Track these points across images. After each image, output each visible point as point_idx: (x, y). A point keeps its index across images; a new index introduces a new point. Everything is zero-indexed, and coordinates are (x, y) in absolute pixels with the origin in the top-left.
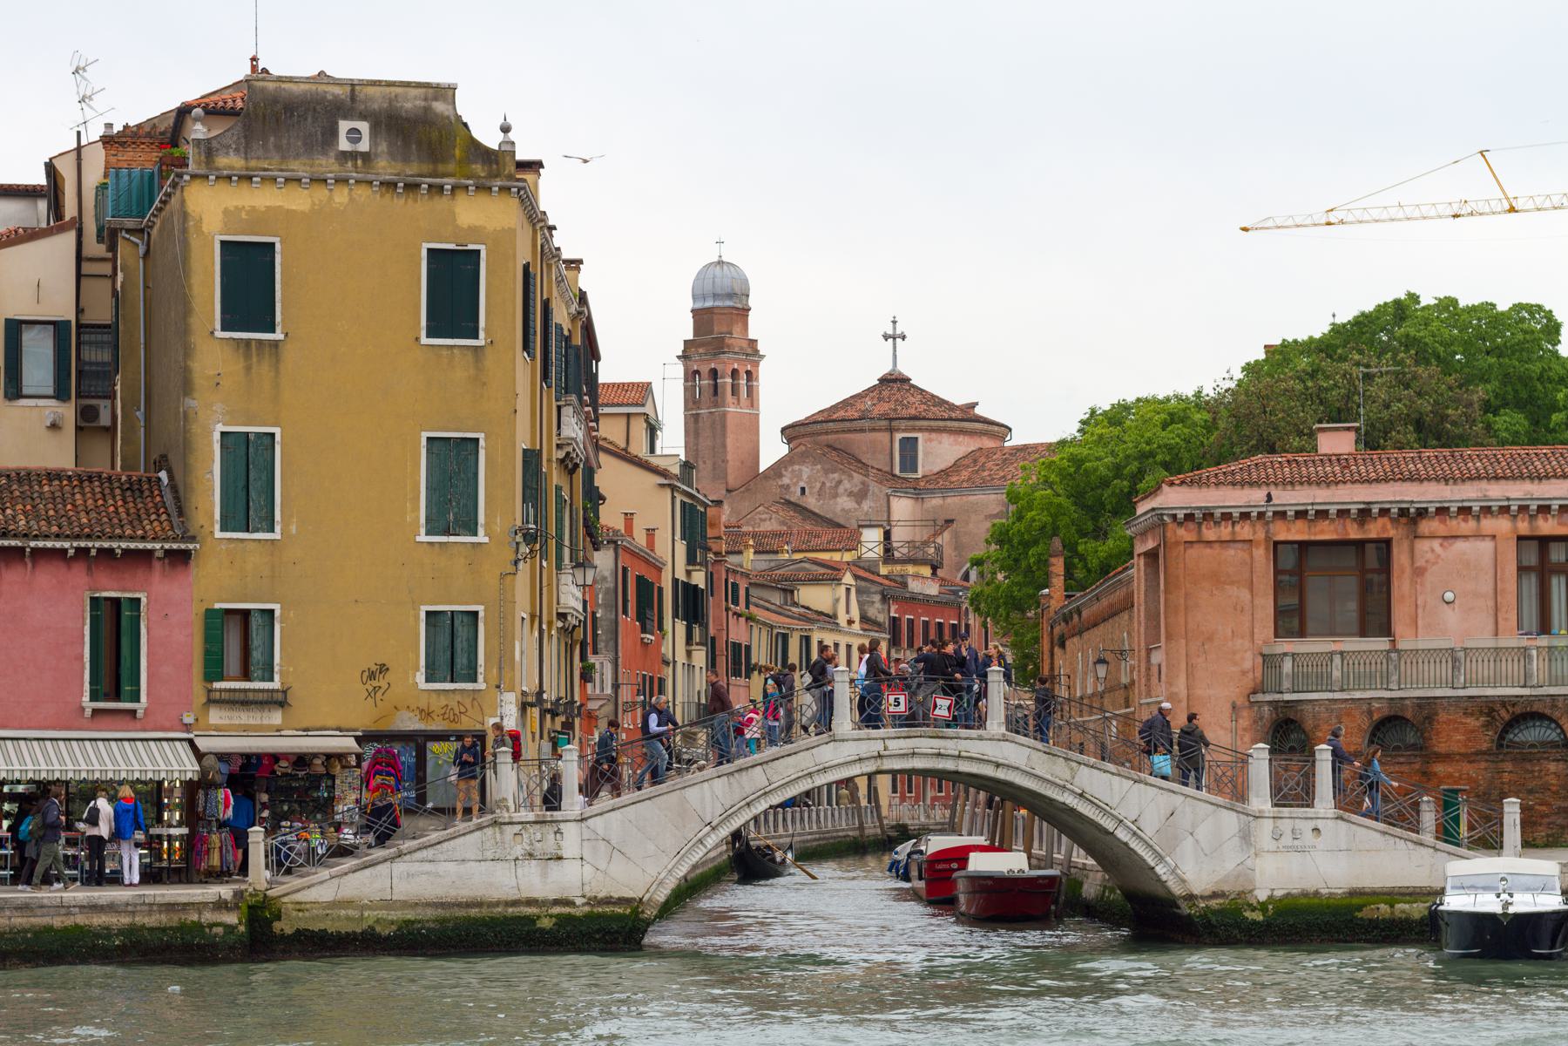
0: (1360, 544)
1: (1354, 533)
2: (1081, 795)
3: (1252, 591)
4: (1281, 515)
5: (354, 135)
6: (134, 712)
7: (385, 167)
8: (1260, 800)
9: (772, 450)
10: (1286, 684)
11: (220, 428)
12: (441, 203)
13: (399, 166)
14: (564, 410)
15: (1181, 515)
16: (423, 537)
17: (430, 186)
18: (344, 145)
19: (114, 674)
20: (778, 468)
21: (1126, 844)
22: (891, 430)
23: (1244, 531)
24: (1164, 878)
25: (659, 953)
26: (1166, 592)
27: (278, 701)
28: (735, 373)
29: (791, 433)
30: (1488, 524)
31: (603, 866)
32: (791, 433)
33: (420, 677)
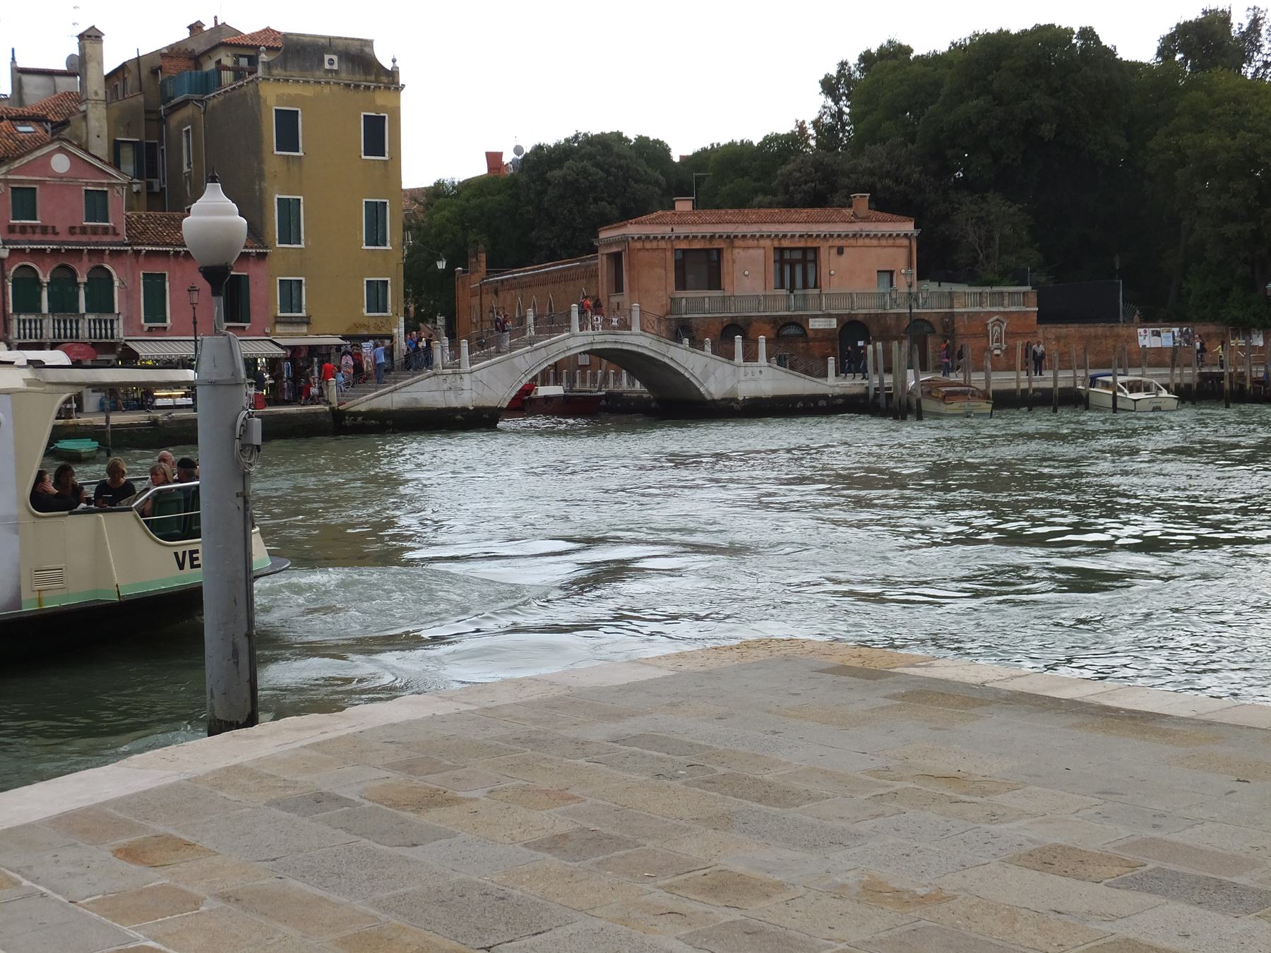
0: (708, 251)
1: (708, 246)
4: (678, 238)
5: (331, 61)
7: (345, 77)
8: (739, 358)
11: (277, 196)
12: (369, 94)
13: (351, 77)
16: (364, 247)
18: (327, 66)
23: (663, 244)
25: (500, 430)
27: (306, 321)
33: (365, 310)
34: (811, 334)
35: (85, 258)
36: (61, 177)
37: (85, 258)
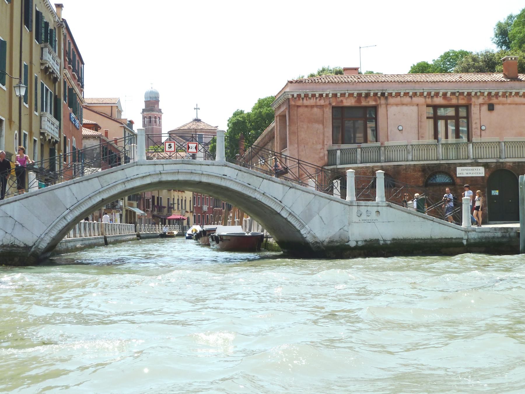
2: (263, 194)
3: (323, 125)
10: (338, 161)
14: (44, 50)
15: (295, 96)
21: (286, 219)
24: (305, 236)
26: (290, 125)
28: (155, 118)
29: (170, 133)
30: (416, 100)
31: (9, 231)
34: (458, 181)
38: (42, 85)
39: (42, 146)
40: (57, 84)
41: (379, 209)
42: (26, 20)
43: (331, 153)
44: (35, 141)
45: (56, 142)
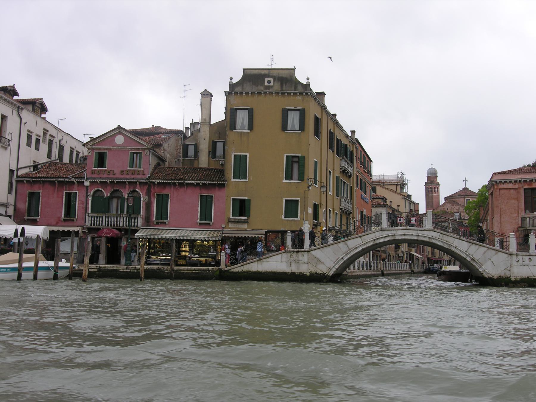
5: (269, 82)
6: (209, 224)
9: (442, 201)
17: (288, 93)
18: (266, 84)
19: (206, 214)
20: (443, 205)
22: (465, 198)
28: (435, 188)
29: (446, 199)
32: (446, 199)
33: (283, 216)
35: (127, 186)
36: (119, 146)
37: (127, 186)
38: (342, 180)
39: (341, 216)
40: (351, 178)
41: (531, 257)
42: (331, 147)
43: (524, 219)
44: (337, 213)
45: (351, 213)
